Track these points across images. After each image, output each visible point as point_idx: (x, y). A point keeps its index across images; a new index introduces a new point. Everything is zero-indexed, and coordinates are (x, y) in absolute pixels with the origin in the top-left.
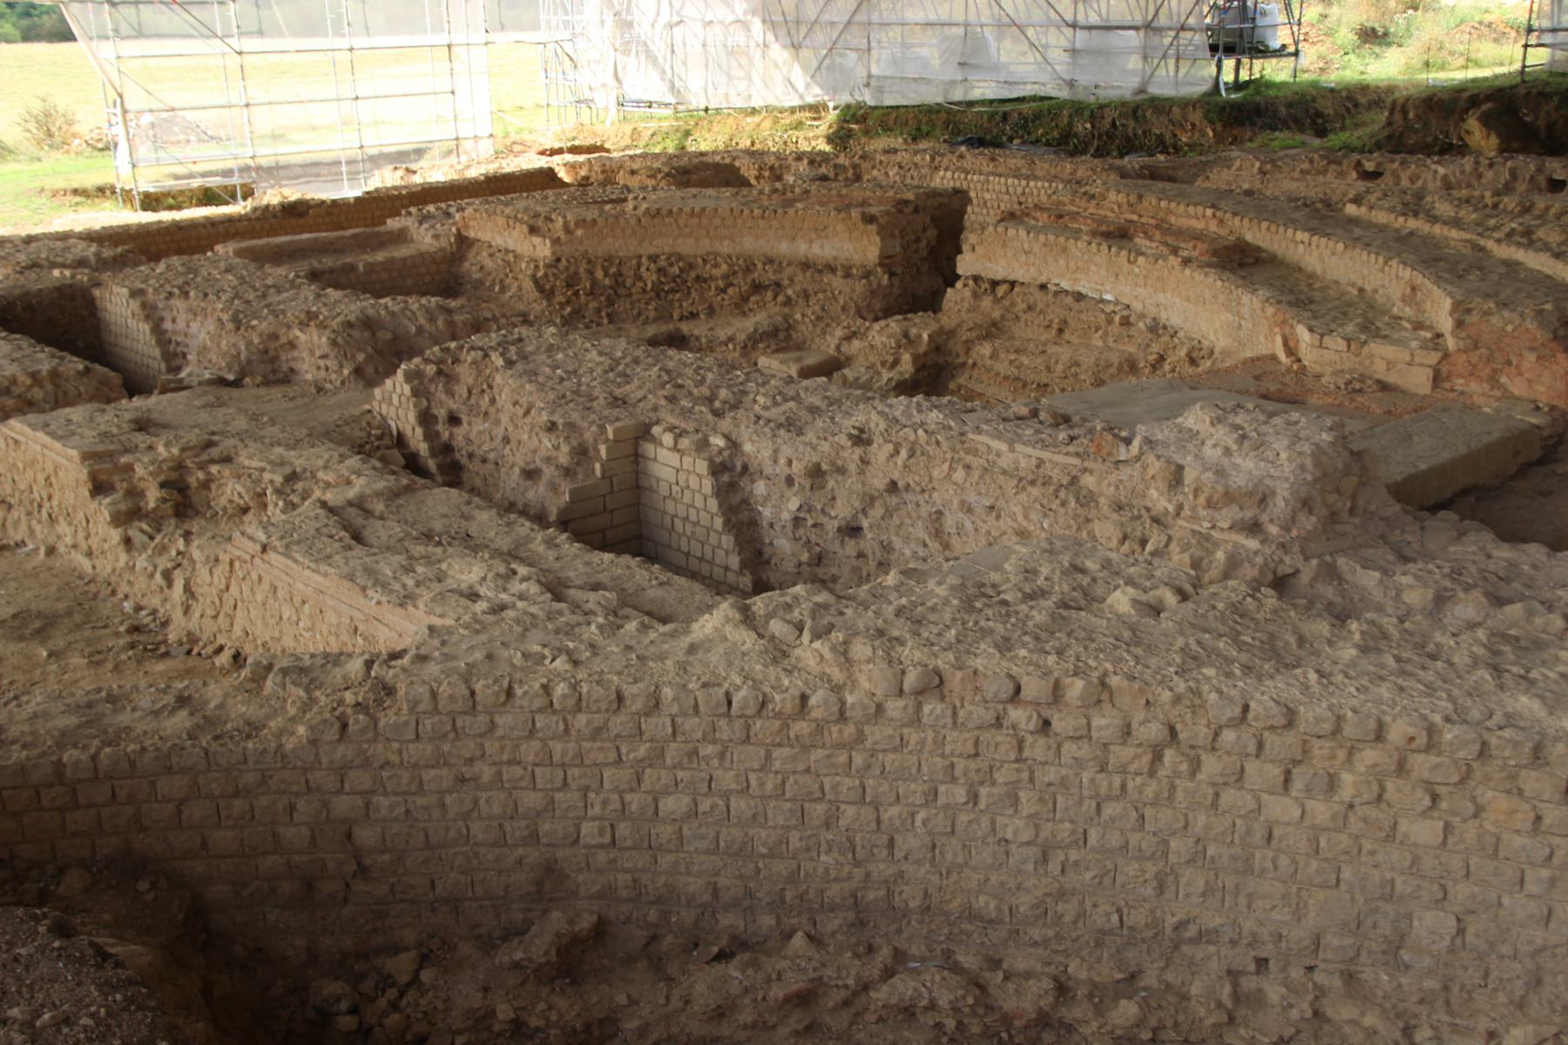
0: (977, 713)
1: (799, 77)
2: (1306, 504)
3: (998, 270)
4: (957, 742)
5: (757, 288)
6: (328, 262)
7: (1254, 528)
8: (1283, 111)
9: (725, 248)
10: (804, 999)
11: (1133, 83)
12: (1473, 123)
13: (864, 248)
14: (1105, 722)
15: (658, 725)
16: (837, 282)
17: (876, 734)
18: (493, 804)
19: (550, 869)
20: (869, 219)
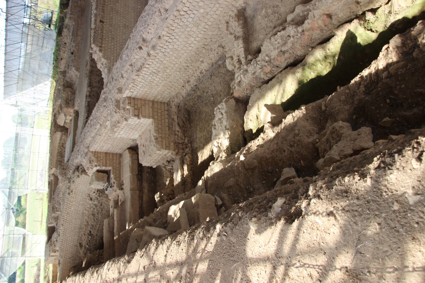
0: (65, 223)
1: (47, 82)
2: (63, 176)
3: (63, 123)
4: (67, 224)
5: (63, 146)
6: (52, 192)
7: (64, 181)
8: (60, 24)
9: (57, 148)
10: (85, 235)
11: (53, 41)
12: (64, 11)
13: (59, 134)
14: (66, 217)
15: (64, 239)
16: (63, 138)
17: (66, 228)
18: (69, 249)
19: (75, 246)
20: (55, 132)
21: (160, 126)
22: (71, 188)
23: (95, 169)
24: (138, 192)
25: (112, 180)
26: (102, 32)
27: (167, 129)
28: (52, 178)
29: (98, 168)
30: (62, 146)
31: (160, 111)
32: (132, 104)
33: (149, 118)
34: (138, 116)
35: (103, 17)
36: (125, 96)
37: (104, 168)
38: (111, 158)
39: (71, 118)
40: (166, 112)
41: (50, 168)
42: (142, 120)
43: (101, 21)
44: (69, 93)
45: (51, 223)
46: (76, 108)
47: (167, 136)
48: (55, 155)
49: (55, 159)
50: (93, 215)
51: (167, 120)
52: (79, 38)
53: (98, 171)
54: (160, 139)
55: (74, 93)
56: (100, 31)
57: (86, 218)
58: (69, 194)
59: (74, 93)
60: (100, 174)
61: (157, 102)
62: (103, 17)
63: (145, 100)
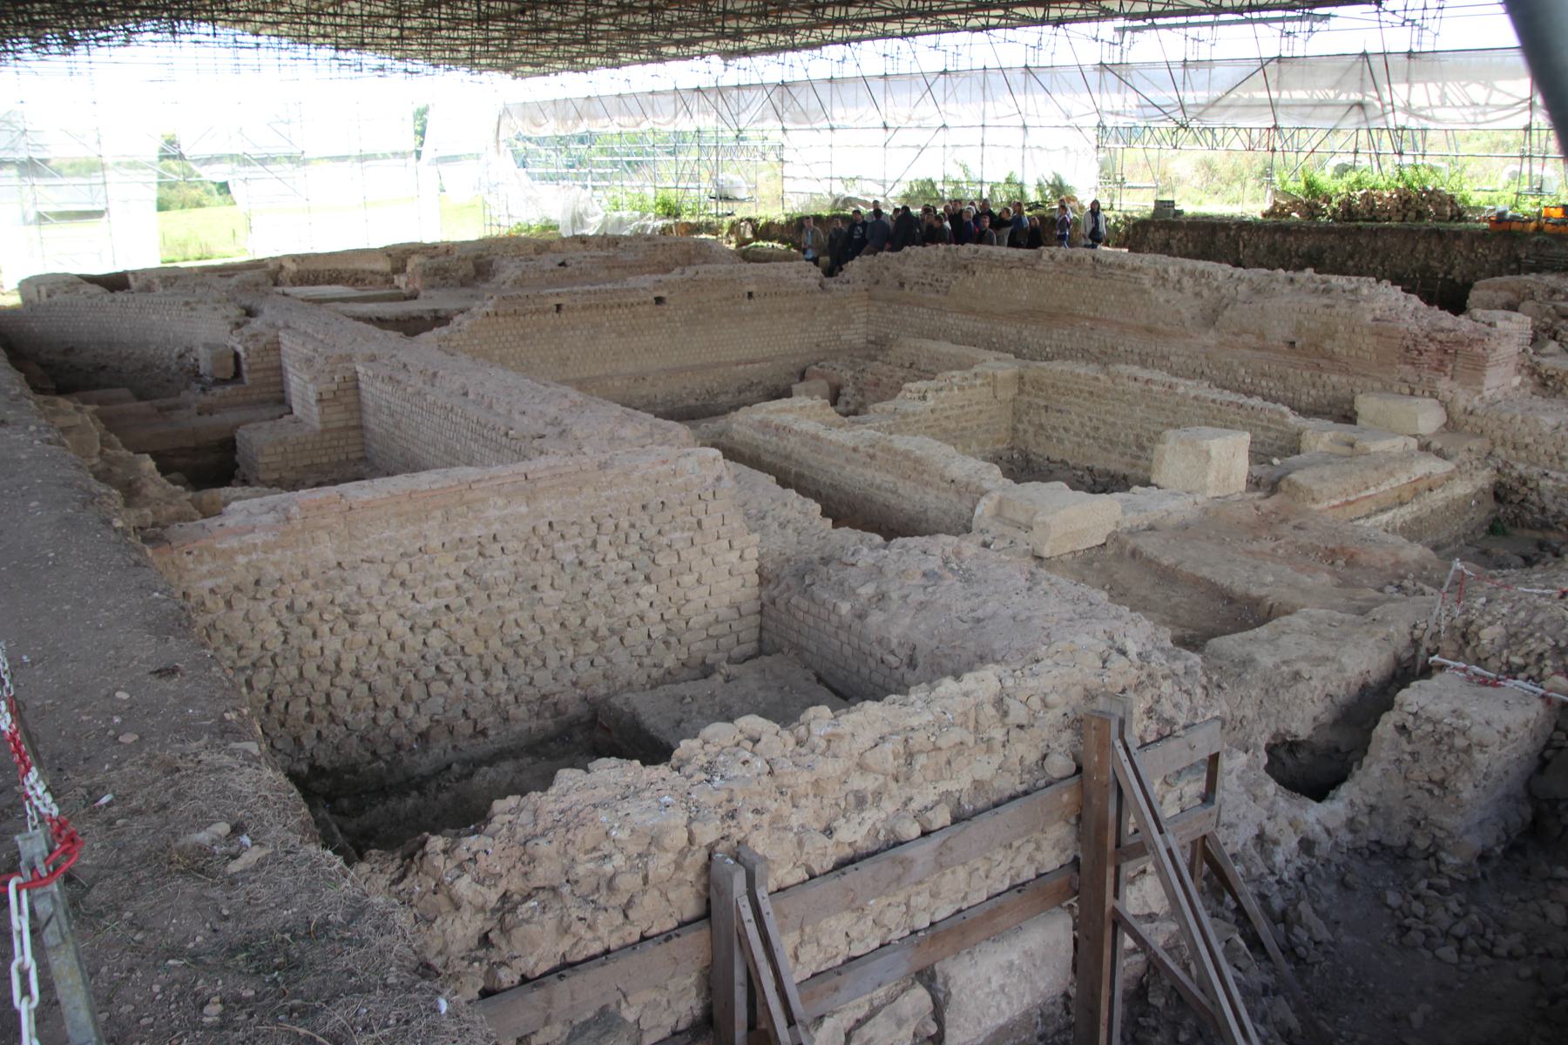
21: (309, 446)
22: (199, 306)
23: (240, 349)
24: (192, 444)
25: (218, 391)
26: (533, 313)
27: (307, 462)
28: (271, 267)
29: (243, 355)
30: (355, 279)
31: (342, 443)
32: (343, 386)
33: (322, 422)
34: (320, 401)
35: (571, 309)
36: (359, 368)
37: (245, 367)
38: (272, 380)
39: (403, 286)
40: (343, 457)
41: (295, 258)
42: (316, 410)
43: (559, 307)
44: (461, 273)
45: (136, 279)
46: (422, 293)
47: (291, 464)
48: (331, 266)
49: (320, 266)
50: (145, 368)
51: (325, 460)
52: (603, 274)
53: (237, 356)
54: (281, 449)
55: (464, 283)
56: (533, 307)
57: (138, 352)
58: (187, 304)
59: (463, 284)
60: (231, 362)
61: (363, 436)
62: (571, 309)
63: (360, 410)
